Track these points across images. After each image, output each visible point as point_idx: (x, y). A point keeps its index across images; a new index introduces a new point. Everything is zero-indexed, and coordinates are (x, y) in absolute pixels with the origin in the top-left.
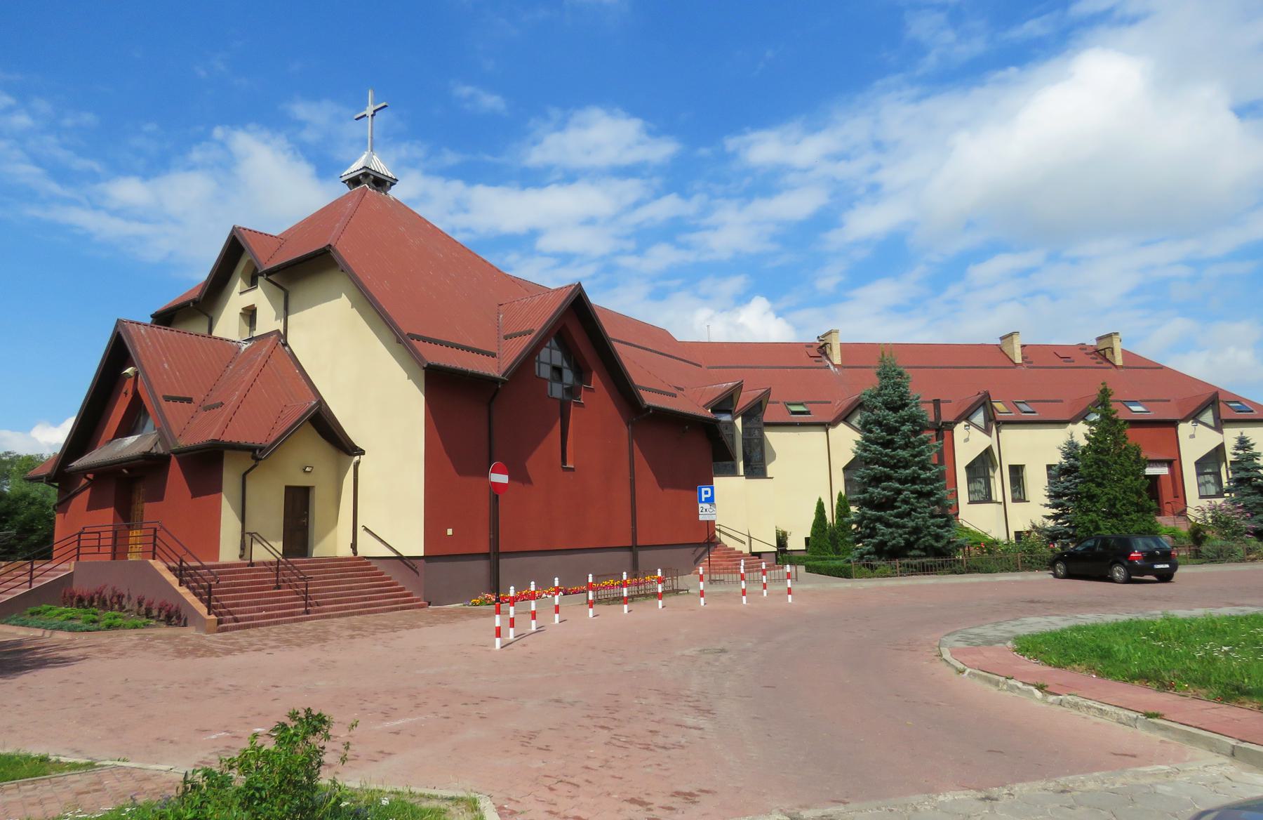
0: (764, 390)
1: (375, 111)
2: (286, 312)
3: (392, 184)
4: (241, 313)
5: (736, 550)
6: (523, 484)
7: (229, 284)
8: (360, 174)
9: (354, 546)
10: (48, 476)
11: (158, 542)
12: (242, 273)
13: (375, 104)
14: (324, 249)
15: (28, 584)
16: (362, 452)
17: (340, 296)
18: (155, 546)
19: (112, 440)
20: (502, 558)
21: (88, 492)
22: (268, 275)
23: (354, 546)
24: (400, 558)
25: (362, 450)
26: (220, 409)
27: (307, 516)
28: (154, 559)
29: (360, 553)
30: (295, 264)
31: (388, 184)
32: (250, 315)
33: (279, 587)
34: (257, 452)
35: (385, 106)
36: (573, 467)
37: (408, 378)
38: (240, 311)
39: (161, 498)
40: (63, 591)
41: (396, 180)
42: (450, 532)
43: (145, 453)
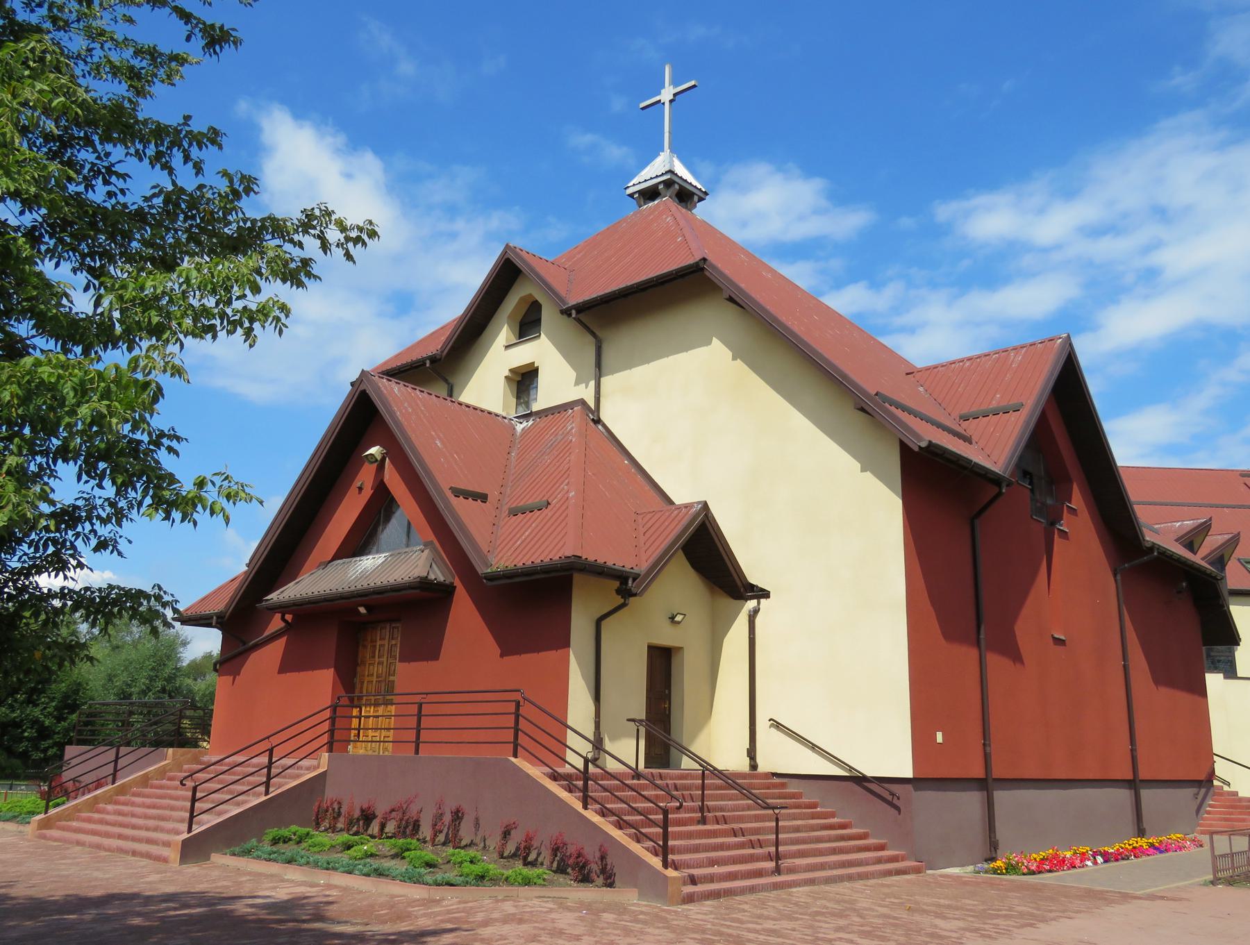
0: (1227, 537)
1: (675, 95)
2: (599, 370)
3: (701, 199)
4: (506, 377)
5: (1240, 795)
6: (1014, 662)
7: (483, 335)
8: (660, 183)
9: (752, 753)
10: (220, 616)
11: (523, 724)
12: (509, 317)
13: (675, 83)
14: (697, 264)
15: (262, 789)
16: (764, 594)
17: (709, 343)
18: (517, 731)
19: (330, 562)
20: (996, 790)
21: (281, 644)
22: (578, 312)
23: (752, 753)
24: (860, 780)
25: (762, 590)
26: (545, 511)
27: (668, 697)
28: (515, 756)
29: (764, 766)
30: (674, 279)
31: (696, 198)
32: (524, 380)
33: (703, 821)
34: (630, 582)
35: (694, 86)
36: (1064, 638)
37: (863, 470)
38: (507, 373)
39: (438, 659)
40: (317, 804)
41: (706, 193)
42: (939, 737)
43: (421, 578)
